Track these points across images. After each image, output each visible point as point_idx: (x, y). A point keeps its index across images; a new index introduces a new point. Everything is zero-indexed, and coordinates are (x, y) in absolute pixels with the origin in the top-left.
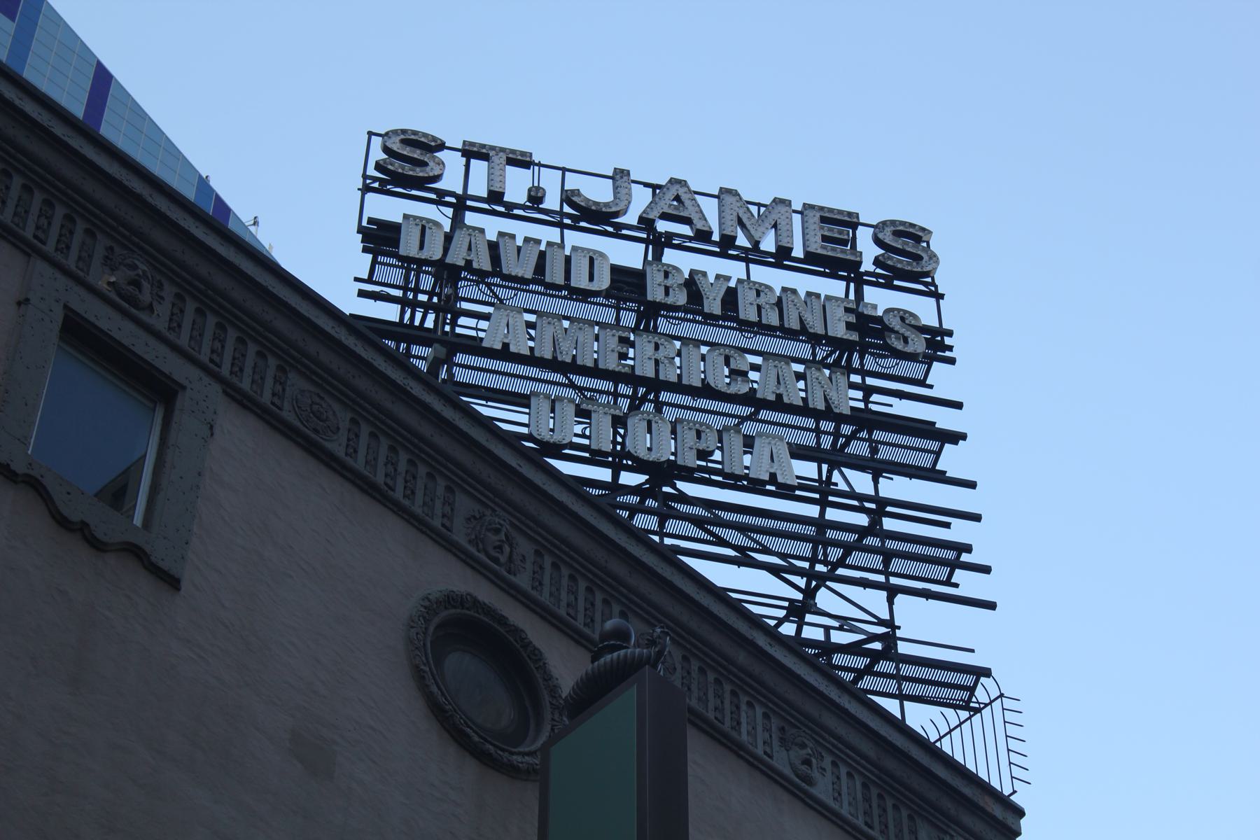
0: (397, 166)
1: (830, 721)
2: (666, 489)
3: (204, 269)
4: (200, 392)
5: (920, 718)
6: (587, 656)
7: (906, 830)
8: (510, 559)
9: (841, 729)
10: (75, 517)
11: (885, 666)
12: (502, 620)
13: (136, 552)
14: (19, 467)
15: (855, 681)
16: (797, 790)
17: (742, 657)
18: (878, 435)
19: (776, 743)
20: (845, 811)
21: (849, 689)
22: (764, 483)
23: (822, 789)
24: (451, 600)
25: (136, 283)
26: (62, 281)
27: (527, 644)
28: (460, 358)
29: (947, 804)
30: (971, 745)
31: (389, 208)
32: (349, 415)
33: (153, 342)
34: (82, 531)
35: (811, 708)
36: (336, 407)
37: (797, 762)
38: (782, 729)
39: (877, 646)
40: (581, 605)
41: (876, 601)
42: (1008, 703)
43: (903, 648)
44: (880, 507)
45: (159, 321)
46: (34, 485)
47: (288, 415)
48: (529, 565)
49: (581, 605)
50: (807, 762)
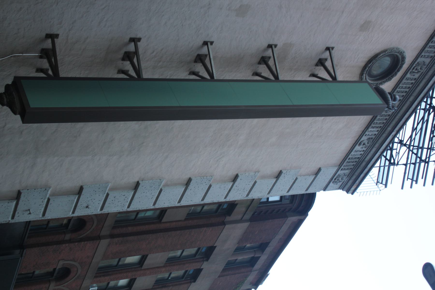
1: (374, 150)
2: (431, 110)
5: (374, 171)
7: (348, 167)
8: (414, 72)
11: (387, 163)
12: (398, 71)
16: (357, 142)
17: (389, 129)
19: (369, 137)
20: (352, 153)
22: (433, 134)
23: (357, 148)
24: (403, 58)
27: (392, 77)
29: (354, 177)
35: (377, 145)
37: (364, 142)
38: (372, 138)
39: (392, 161)
41: (403, 161)
43: (392, 167)
48: (412, 77)
50: (364, 144)
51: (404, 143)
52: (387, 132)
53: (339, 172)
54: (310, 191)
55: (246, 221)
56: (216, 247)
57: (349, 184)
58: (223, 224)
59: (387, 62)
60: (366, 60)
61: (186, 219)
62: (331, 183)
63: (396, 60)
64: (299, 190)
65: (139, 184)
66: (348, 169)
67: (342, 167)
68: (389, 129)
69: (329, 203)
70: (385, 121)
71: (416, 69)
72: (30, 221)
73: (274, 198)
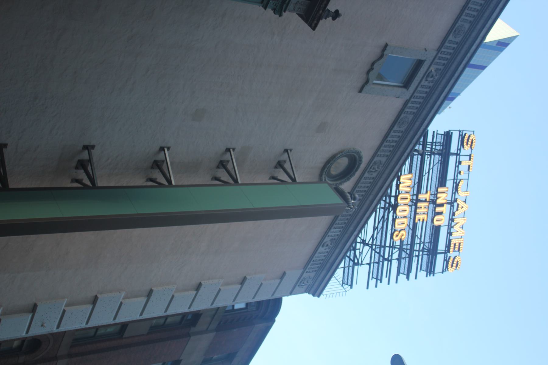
1: (337, 251)
2: (391, 209)
5: (339, 273)
6: (349, 191)
8: (371, 171)
10: (375, 66)
11: (351, 263)
12: (356, 170)
13: (367, 82)
14: (385, 53)
16: (321, 243)
17: (351, 228)
18: (407, 259)
19: (331, 238)
20: (316, 255)
23: (321, 249)
24: (360, 158)
25: (432, 76)
26: (432, 59)
27: (351, 177)
28: (420, 157)
30: (334, 284)
33: (418, 81)
34: (371, 69)
35: (340, 246)
36: (406, 127)
39: (356, 261)
40: (361, 189)
41: (367, 260)
42: (344, 293)
43: (356, 267)
44: (390, 261)
45: (424, 83)
46: (382, 56)
47: (403, 116)
48: (370, 176)
49: (361, 189)
51: (367, 242)
52: (349, 232)
54: (276, 296)
56: (181, 360)
57: (315, 287)
58: (188, 335)
59: (343, 162)
60: (325, 161)
63: (354, 160)
67: (307, 270)
68: (351, 228)
69: (294, 308)
71: (374, 169)
73: (240, 305)
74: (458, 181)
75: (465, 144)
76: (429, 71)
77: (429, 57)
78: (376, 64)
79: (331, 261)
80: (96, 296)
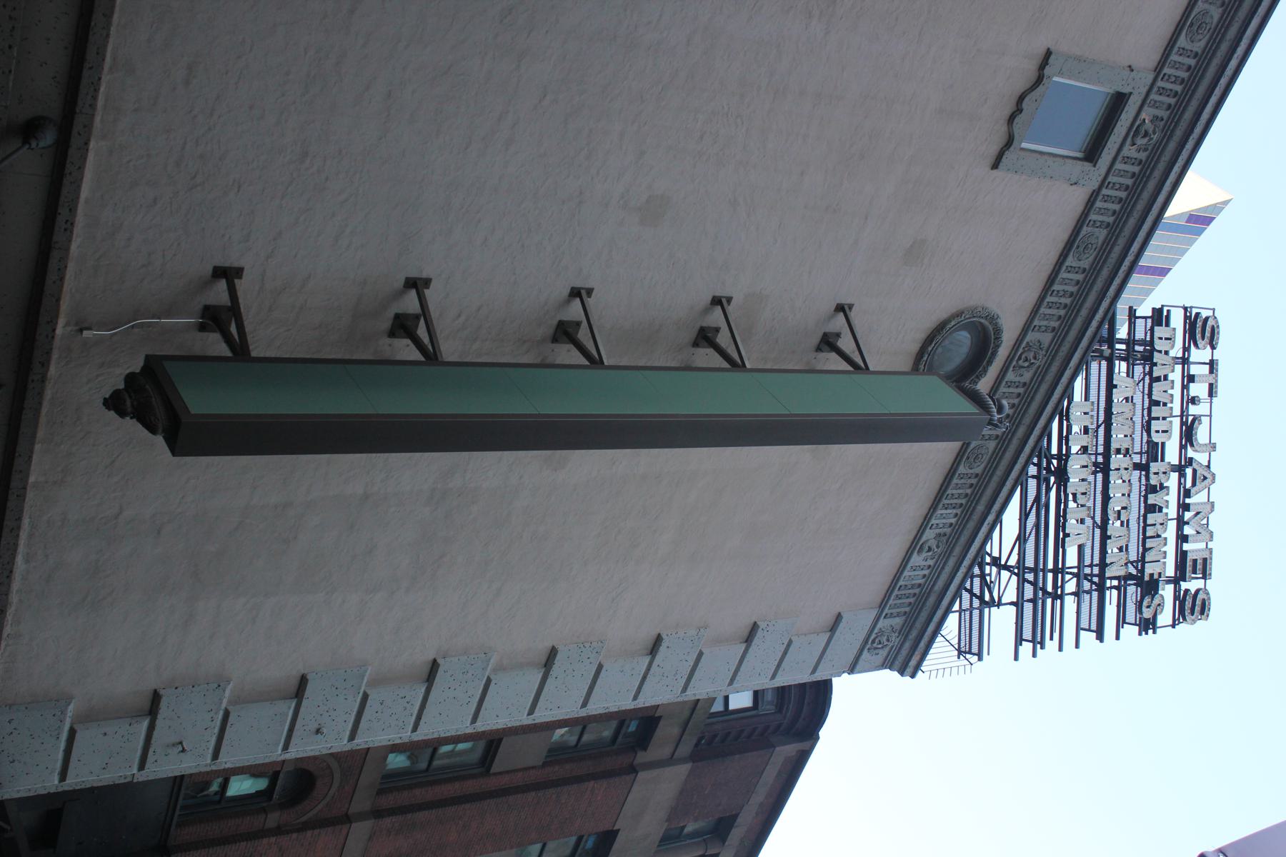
0: (1199, 324)
1: (951, 562)
2: (1052, 479)
3: (1157, 174)
4: (1094, 175)
9: (948, 569)
10: (1024, 105)
11: (976, 603)
12: (990, 363)
14: (1047, 71)
15: (966, 590)
16: (915, 545)
17: (980, 508)
18: (1095, 594)
19: (938, 531)
20: (906, 573)
21: (961, 586)
22: (1064, 530)
23: (917, 560)
24: (998, 331)
26: (1144, 90)
28: (1104, 363)
29: (914, 634)
30: (941, 651)
31: (1177, 321)
32: (1087, 267)
33: (1117, 146)
34: (1018, 110)
35: (957, 550)
39: (987, 598)
41: (1011, 595)
43: (986, 610)
44: (1058, 596)
45: (1129, 151)
46: (1039, 80)
48: (1018, 379)
52: (976, 517)
53: (880, 625)
54: (819, 676)
55: (683, 761)
57: (904, 652)
58: (633, 770)
59: (962, 343)
61: (545, 764)
62: (866, 651)
63: (984, 339)
64: (795, 675)
65: (438, 665)
66: (898, 615)
67: (886, 611)
68: (980, 508)
69: (861, 699)
70: (969, 491)
71: (1026, 360)
72: (182, 777)
73: (741, 700)
74: (1190, 418)
75: (1198, 336)
76: (1138, 123)
77: (1137, 86)
78: (1026, 100)
79: (940, 584)
80: (435, 661)
